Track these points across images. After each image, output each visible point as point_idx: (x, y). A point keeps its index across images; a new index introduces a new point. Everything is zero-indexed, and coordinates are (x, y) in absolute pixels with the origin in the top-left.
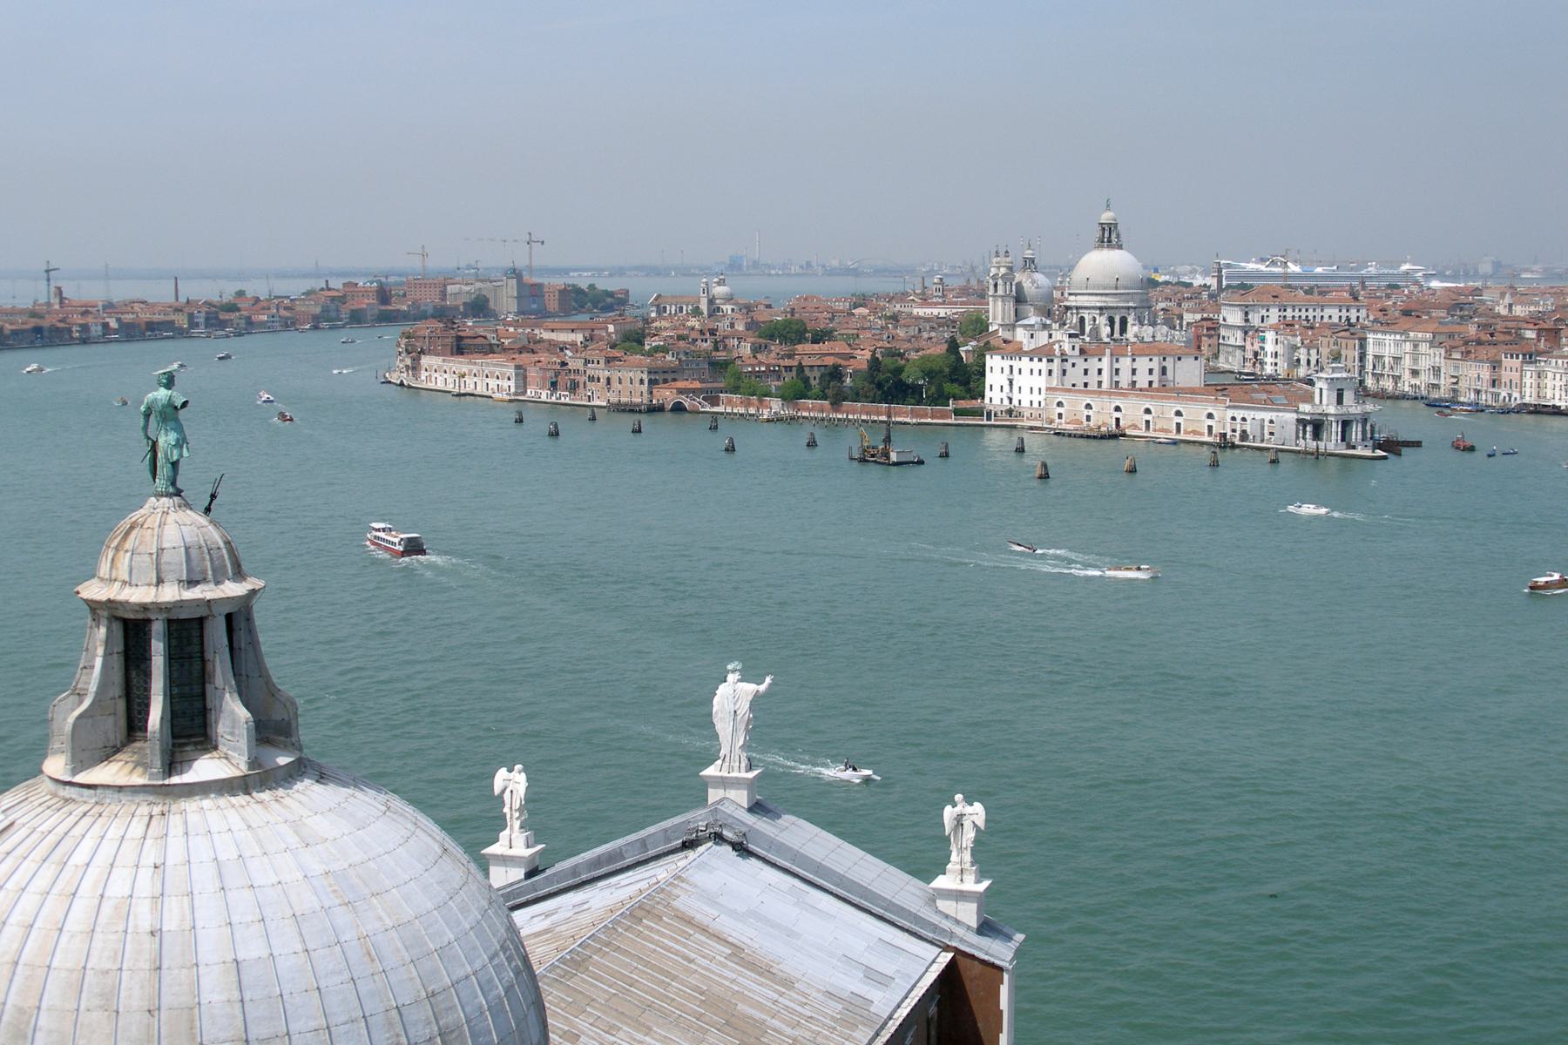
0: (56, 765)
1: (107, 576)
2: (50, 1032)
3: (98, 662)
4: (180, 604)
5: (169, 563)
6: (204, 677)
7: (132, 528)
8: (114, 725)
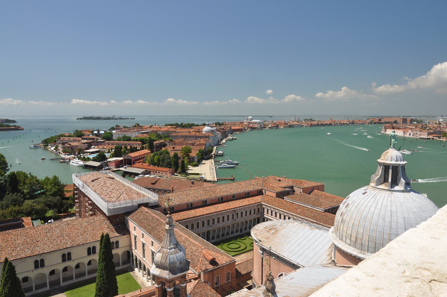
0: (372, 184)
2: (374, 222)
3: (381, 171)
4: (395, 164)
5: (393, 158)
6: (397, 175)
7: (387, 153)
8: (382, 180)
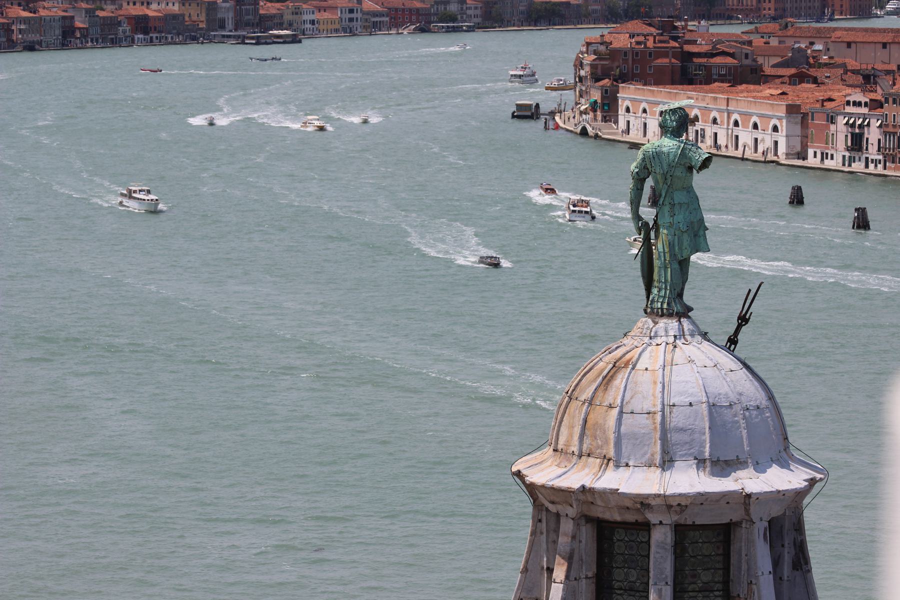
1: (575, 449)
4: (702, 499)
5: (682, 430)
7: (616, 367)
